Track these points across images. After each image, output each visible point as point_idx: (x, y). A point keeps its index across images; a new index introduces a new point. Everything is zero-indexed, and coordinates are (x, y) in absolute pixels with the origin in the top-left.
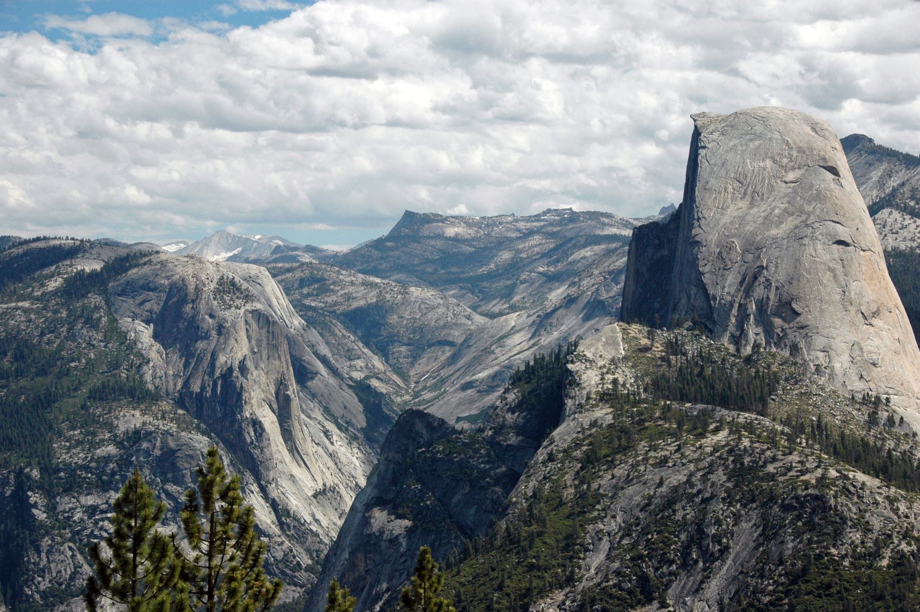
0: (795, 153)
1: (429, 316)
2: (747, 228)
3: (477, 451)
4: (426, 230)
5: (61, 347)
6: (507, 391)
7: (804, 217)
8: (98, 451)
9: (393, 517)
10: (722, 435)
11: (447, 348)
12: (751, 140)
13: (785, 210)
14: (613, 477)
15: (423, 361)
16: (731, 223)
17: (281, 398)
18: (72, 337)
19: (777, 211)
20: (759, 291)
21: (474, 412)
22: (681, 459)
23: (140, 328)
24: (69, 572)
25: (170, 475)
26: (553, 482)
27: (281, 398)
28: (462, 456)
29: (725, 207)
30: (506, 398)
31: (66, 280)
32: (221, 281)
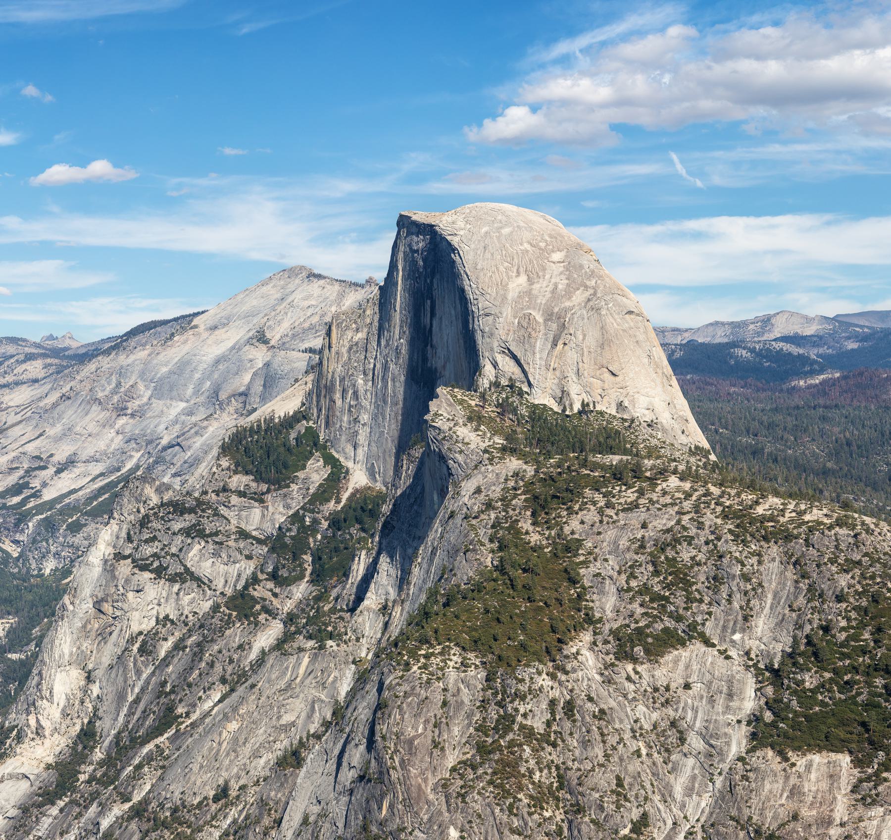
2: (539, 301)
3: (203, 511)
12: (501, 228)
16: (519, 297)
22: (653, 505)
29: (504, 284)
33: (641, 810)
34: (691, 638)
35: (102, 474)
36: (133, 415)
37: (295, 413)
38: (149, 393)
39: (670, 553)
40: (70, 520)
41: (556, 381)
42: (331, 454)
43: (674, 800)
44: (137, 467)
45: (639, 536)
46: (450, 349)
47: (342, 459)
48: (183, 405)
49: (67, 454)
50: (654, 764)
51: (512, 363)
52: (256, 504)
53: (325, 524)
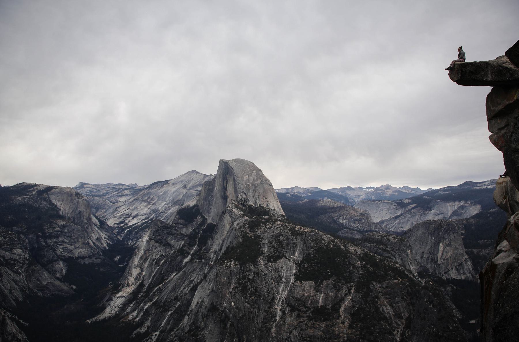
0: (252, 167)
1: (99, 203)
3: (172, 228)
4: (85, 186)
5: (39, 206)
6: (176, 215)
7: (261, 180)
8: (55, 229)
9: (155, 243)
10: (279, 222)
11: (104, 209)
13: (257, 178)
14: (260, 231)
15: (99, 212)
16: (246, 180)
17: (89, 219)
18: (41, 204)
19: (255, 178)
20: (257, 194)
21: (117, 222)
23: (57, 202)
24: (51, 256)
25: (72, 235)
26: (244, 233)
27: (89, 219)
28: (169, 229)
30: (176, 217)
31: (37, 192)
32: (76, 193)
33: (273, 296)
34: (284, 257)
35: (144, 219)
36: (153, 205)
37: (195, 205)
38: (157, 199)
39: (278, 238)
40: (136, 231)
41: (254, 199)
42: (203, 215)
43: (279, 293)
44: (153, 218)
45: (272, 234)
46: (231, 191)
47: (205, 216)
48: (165, 202)
49: (135, 214)
50: (275, 285)
51: (244, 195)
52: (185, 227)
53: (201, 232)
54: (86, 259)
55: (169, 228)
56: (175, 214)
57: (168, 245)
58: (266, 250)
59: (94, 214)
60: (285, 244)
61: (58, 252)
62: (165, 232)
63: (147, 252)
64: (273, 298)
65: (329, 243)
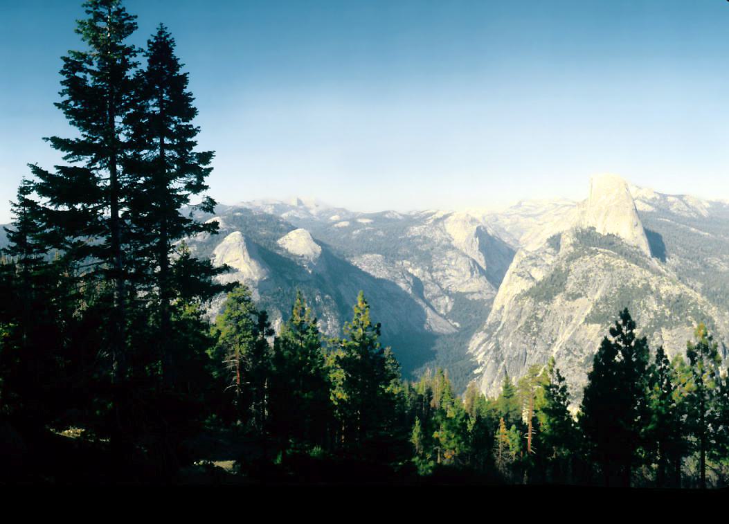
10: (601, 255)
54: (475, 294)
55: (534, 259)
56: (545, 241)
57: (533, 279)
58: (570, 286)
59: (517, 239)
60: (590, 282)
61: (444, 287)
62: (530, 263)
63: (509, 286)
64: (556, 340)
65: (638, 282)
